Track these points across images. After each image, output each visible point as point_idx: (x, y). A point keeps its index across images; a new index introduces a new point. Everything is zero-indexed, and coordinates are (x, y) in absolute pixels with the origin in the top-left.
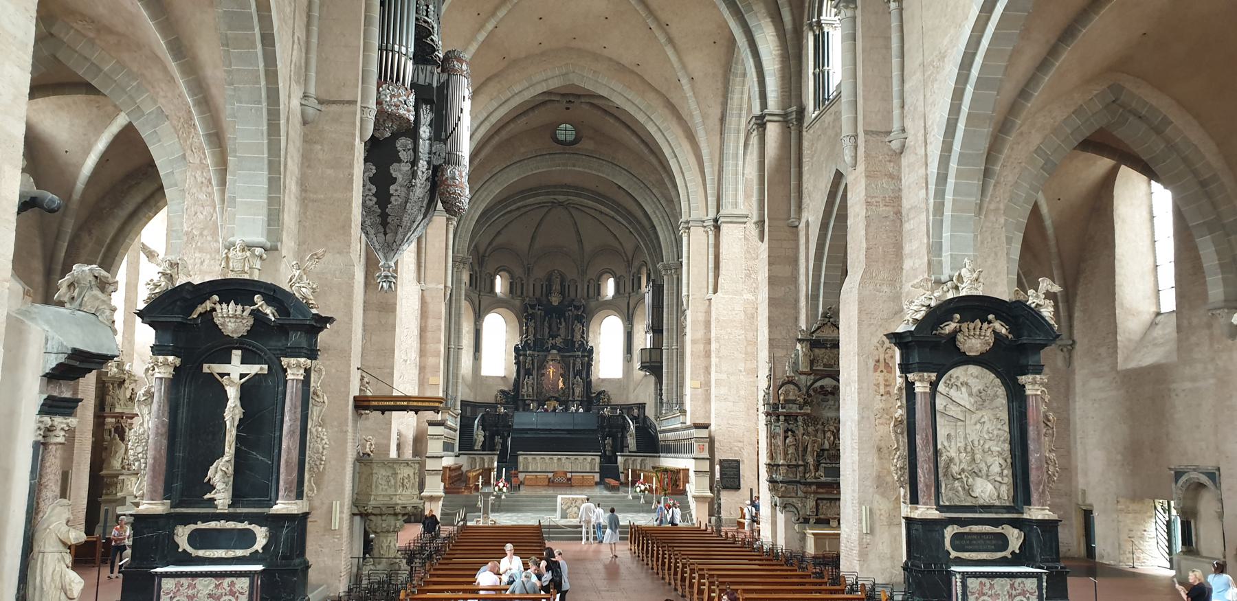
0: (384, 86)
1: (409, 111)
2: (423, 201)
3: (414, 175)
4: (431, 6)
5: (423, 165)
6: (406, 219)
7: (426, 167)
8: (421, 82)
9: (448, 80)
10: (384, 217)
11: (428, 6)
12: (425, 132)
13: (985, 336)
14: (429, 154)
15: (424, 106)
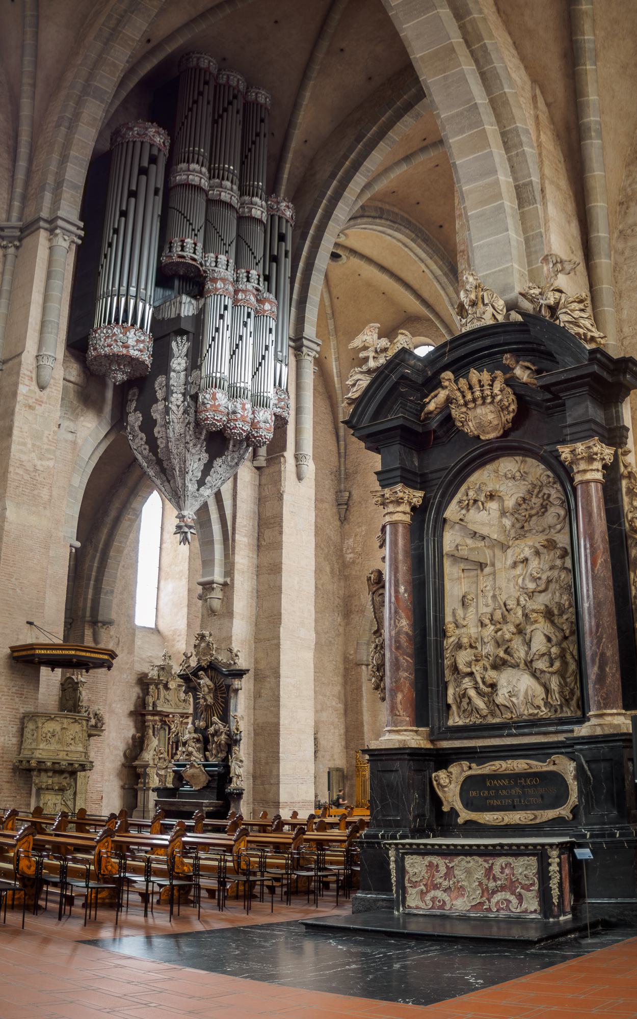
0: (99, 331)
1: (127, 347)
2: (185, 436)
3: (167, 410)
4: (189, 241)
5: (177, 398)
6: (176, 462)
7: (182, 399)
8: (173, 316)
9: (204, 305)
10: (159, 462)
11: (183, 241)
12: (179, 363)
13: (493, 397)
14: (185, 385)
15: (179, 339)
